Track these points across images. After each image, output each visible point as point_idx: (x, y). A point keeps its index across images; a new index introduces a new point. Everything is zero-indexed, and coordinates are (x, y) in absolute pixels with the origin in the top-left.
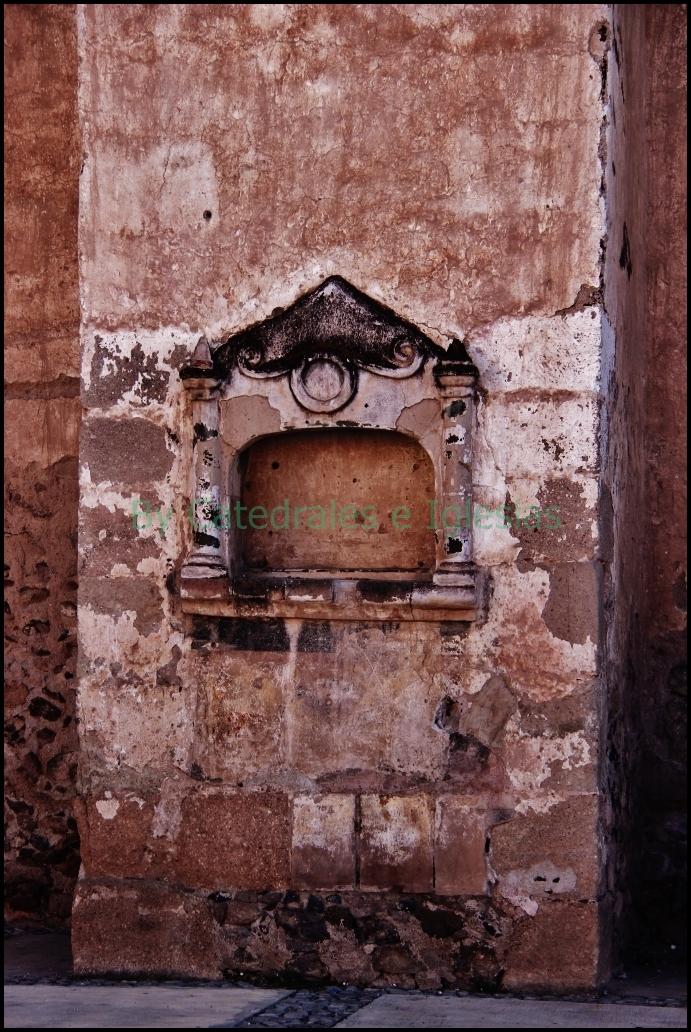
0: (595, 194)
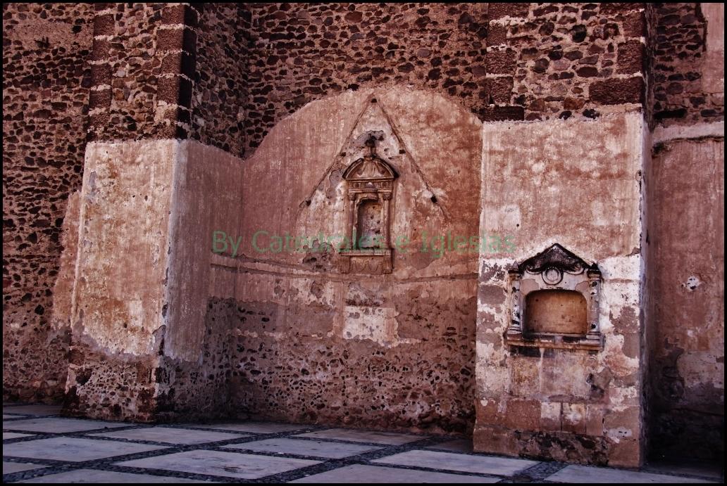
0: (638, 220)
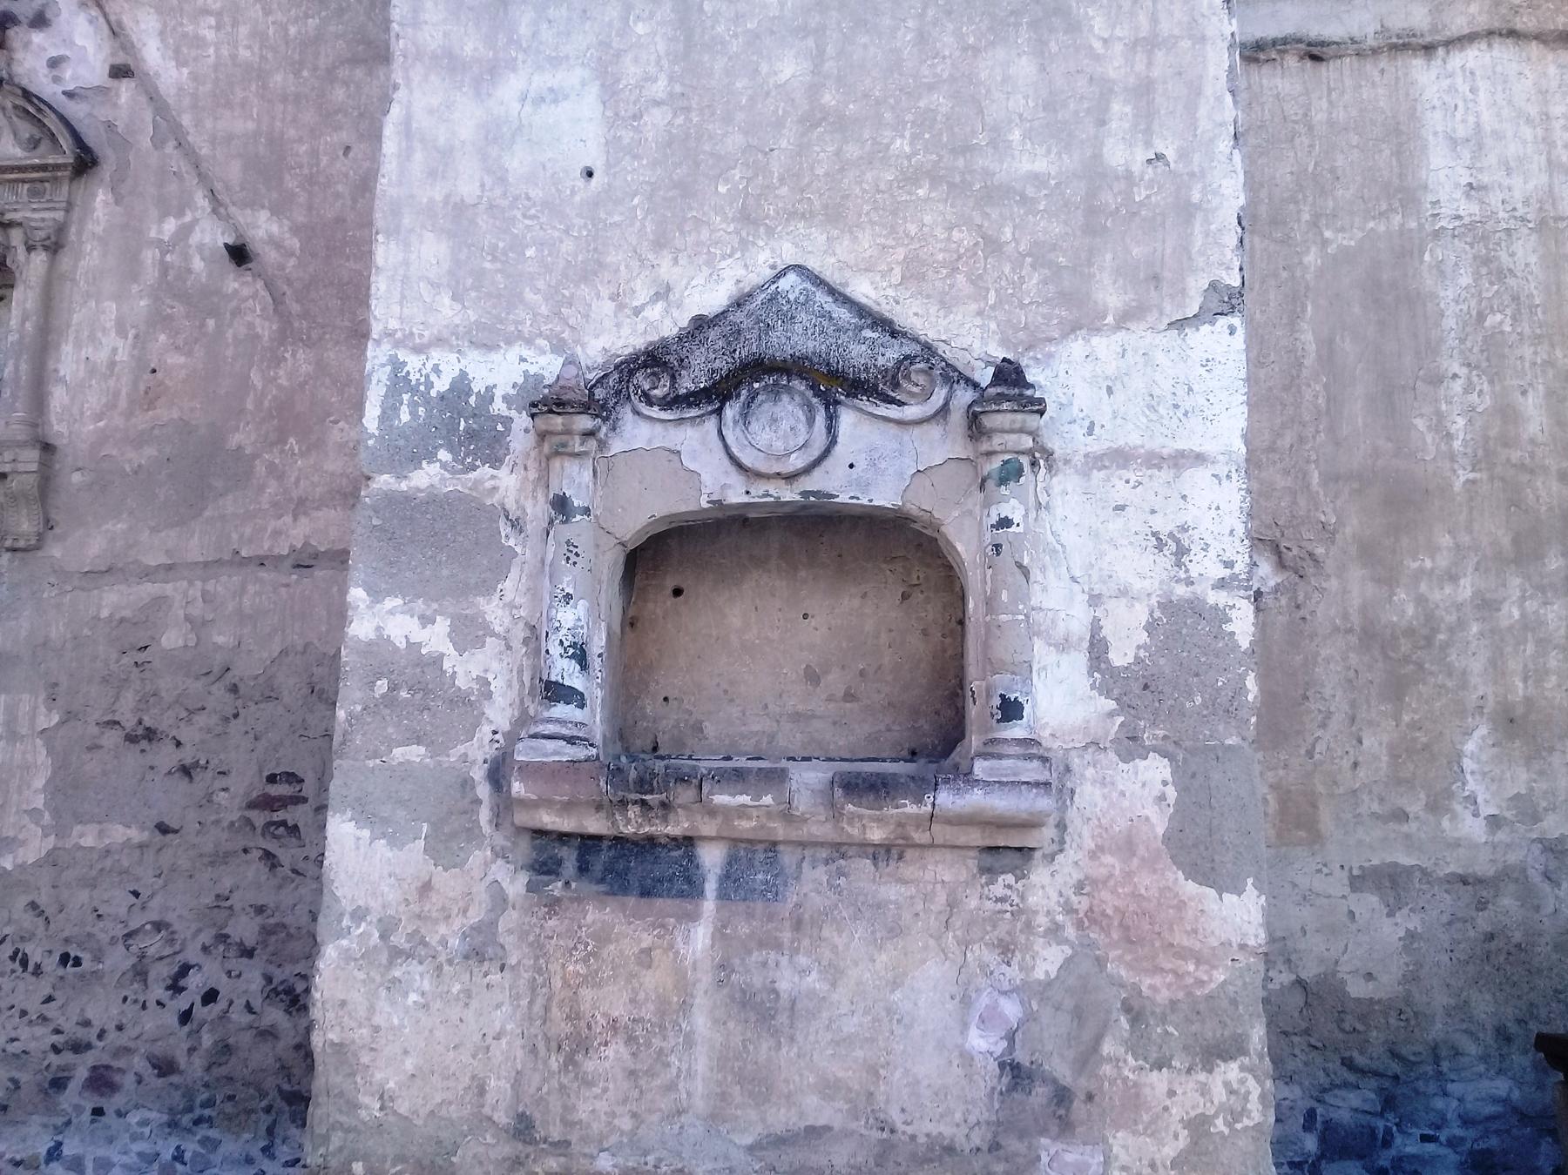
0: (1224, 144)
